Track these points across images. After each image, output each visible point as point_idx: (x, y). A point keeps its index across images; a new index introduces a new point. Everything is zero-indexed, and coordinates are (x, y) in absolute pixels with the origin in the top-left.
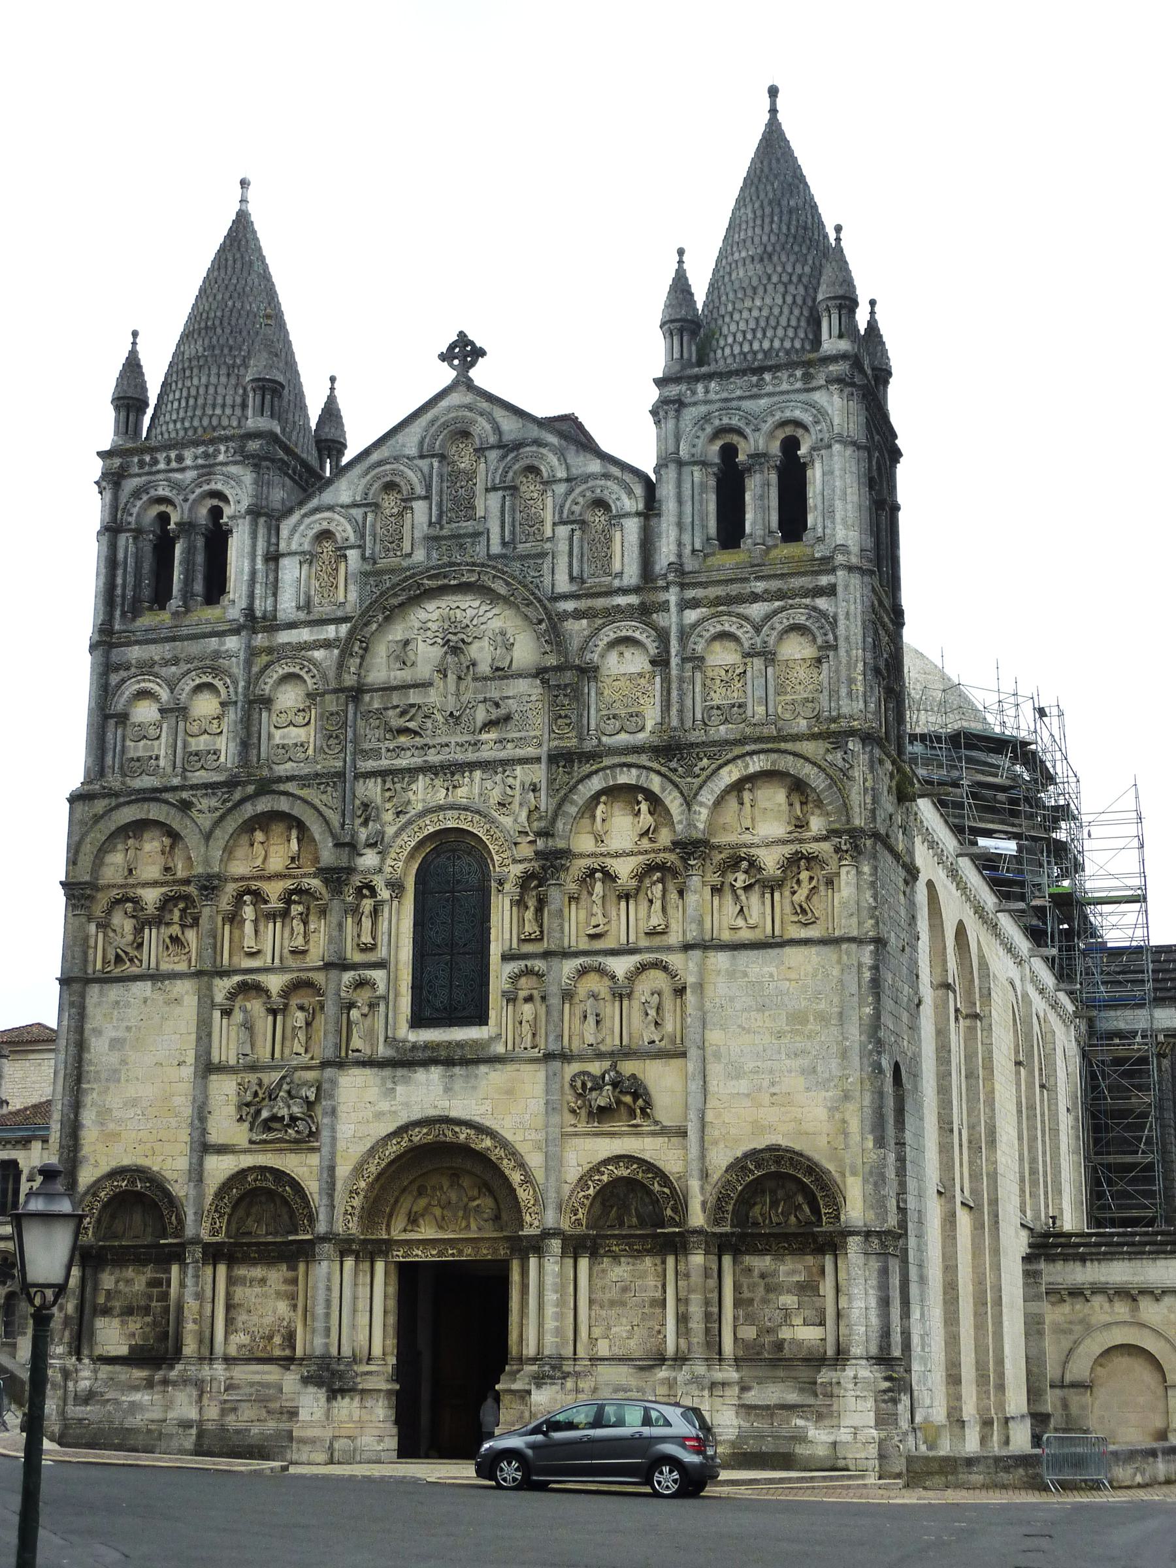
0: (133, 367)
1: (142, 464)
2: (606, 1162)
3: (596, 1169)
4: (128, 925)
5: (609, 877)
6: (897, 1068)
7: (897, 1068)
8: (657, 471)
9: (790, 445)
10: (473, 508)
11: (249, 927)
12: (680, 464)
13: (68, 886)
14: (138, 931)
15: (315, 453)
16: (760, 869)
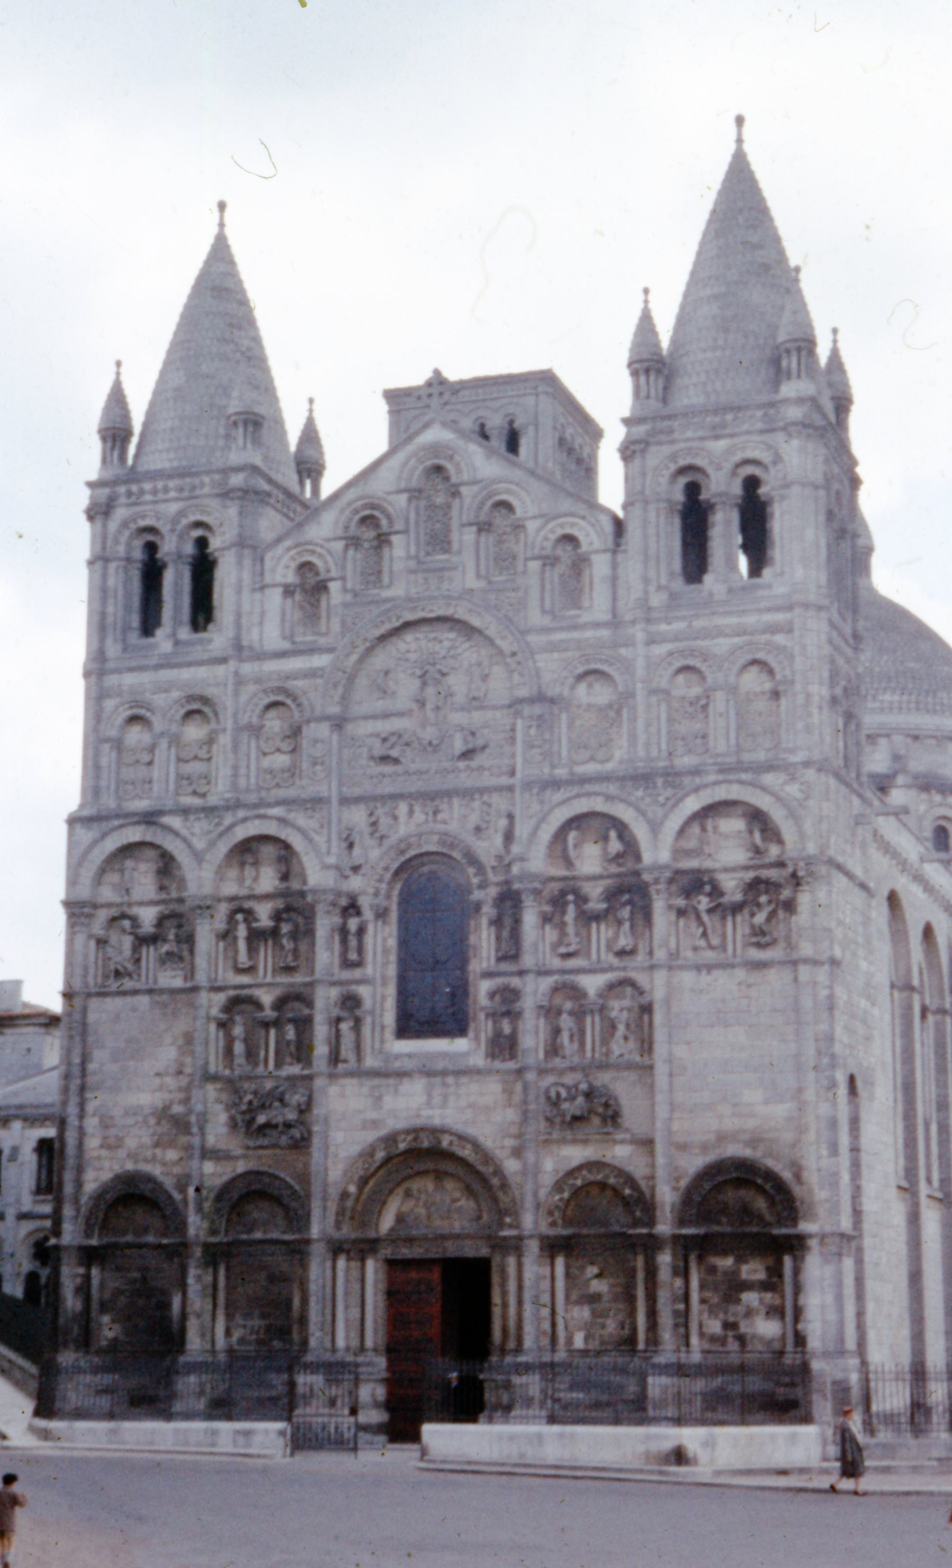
0: (117, 398)
1: (129, 494)
2: (580, 1168)
3: (571, 1173)
4: (127, 942)
5: (581, 899)
6: (852, 1080)
7: (852, 1080)
8: (625, 507)
9: (752, 484)
10: (449, 543)
11: (242, 945)
12: (646, 502)
13: (68, 904)
14: (136, 949)
15: (295, 477)
16: (722, 894)
